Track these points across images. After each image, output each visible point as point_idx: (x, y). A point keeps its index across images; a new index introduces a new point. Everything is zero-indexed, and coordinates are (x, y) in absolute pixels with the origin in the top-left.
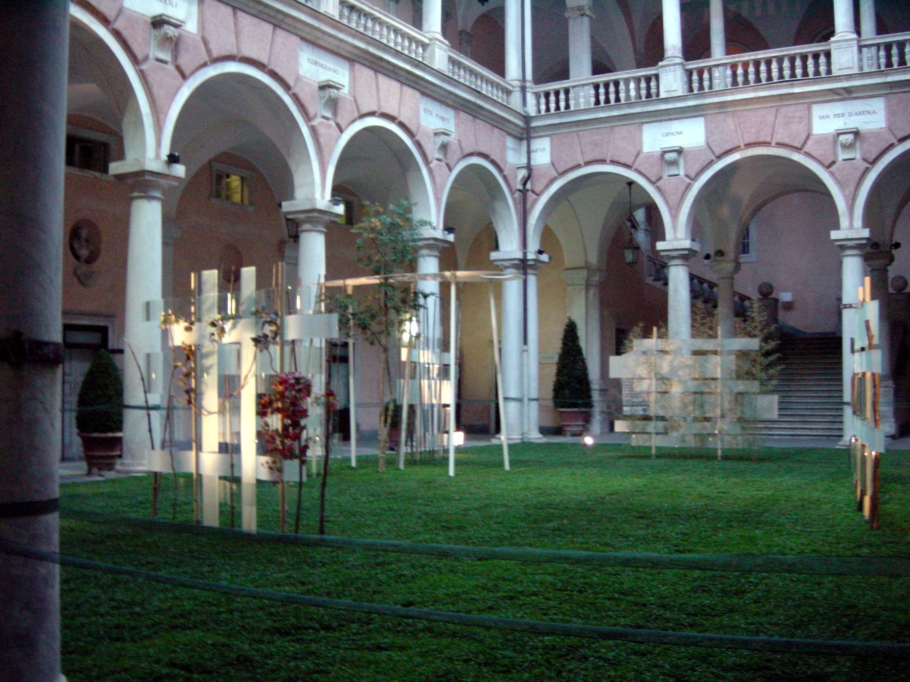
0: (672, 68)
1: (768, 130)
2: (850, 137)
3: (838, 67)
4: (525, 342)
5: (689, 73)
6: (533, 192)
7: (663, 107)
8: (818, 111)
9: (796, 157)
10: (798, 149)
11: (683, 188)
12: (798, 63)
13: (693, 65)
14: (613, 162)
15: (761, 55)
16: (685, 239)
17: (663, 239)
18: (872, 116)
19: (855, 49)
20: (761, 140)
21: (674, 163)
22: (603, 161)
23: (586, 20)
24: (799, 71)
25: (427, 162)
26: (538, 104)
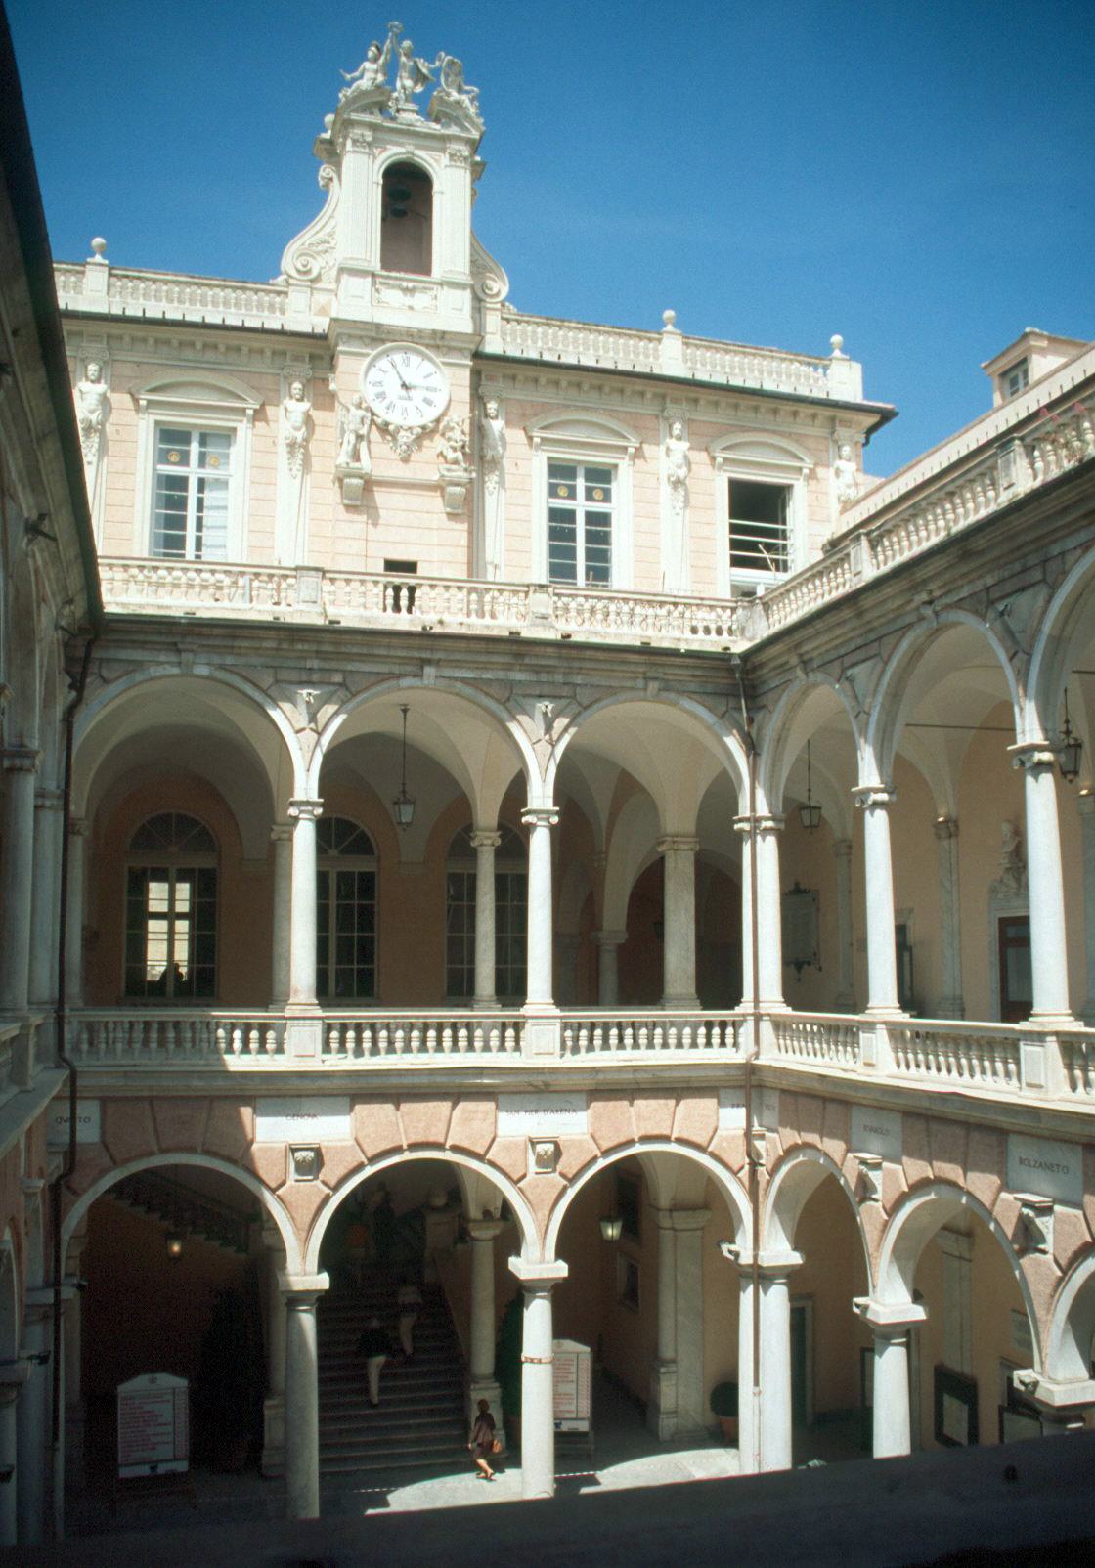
1: (442, 1127)
4: (55, 1437)
9: (474, 1164)
10: (480, 1157)
11: (317, 1201)
14: (208, 1152)
20: (432, 1139)
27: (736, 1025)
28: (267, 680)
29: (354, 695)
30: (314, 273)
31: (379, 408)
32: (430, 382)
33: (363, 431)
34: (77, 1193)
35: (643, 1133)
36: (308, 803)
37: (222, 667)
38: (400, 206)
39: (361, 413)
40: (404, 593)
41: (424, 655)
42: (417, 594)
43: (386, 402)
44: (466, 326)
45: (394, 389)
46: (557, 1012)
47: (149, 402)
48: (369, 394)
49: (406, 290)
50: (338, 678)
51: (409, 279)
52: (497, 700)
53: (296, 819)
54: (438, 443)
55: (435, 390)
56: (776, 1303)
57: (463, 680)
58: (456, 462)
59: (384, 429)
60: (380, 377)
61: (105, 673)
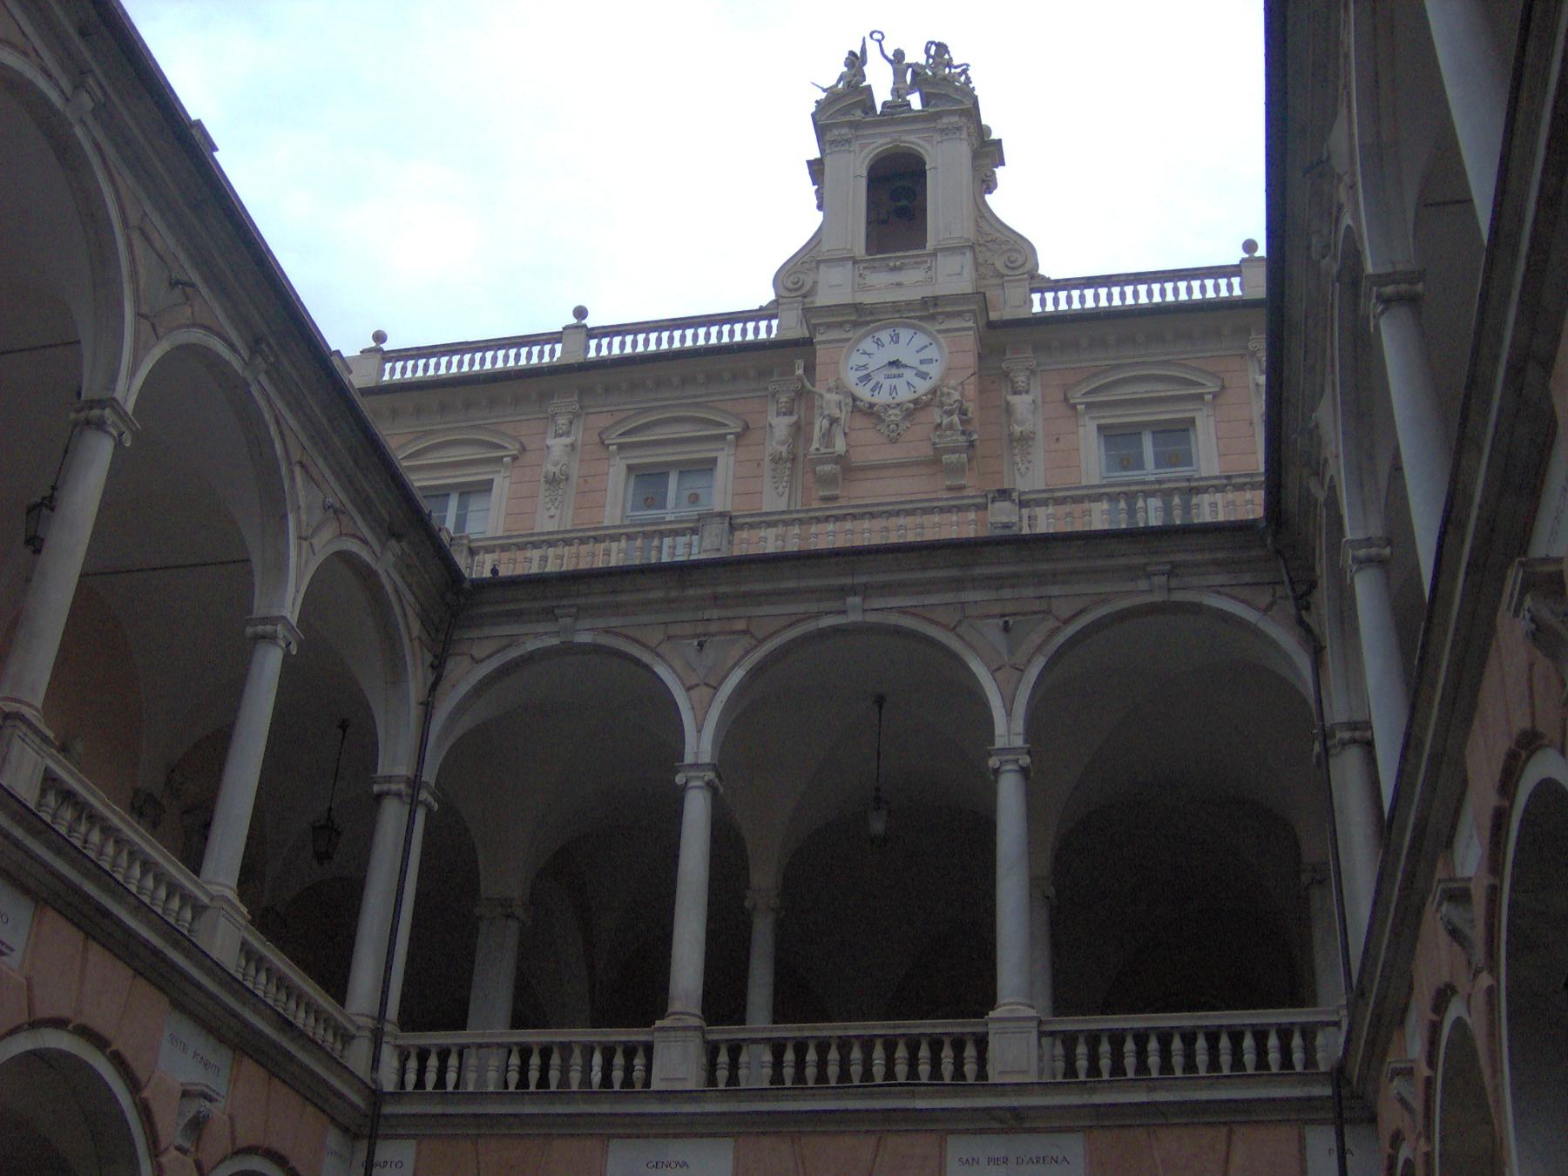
0: (679, 1034)
5: (712, 1050)
7: (655, 1108)
12: (924, 1052)
13: (721, 1033)
15: (856, 1029)
19: (1034, 1034)
23: (514, 925)
24: (924, 1069)
25: (155, 1149)
26: (403, 1072)
28: (654, 637)
29: (761, 642)
30: (807, 288)
31: (864, 393)
33: (843, 416)
36: (696, 766)
37: (607, 631)
38: (904, 203)
41: (847, 581)
44: (965, 285)
47: (621, 447)
48: (851, 378)
49: (894, 269)
52: (945, 626)
54: (936, 415)
55: (930, 361)
57: (903, 611)
59: (870, 412)
60: (863, 360)
61: (478, 652)
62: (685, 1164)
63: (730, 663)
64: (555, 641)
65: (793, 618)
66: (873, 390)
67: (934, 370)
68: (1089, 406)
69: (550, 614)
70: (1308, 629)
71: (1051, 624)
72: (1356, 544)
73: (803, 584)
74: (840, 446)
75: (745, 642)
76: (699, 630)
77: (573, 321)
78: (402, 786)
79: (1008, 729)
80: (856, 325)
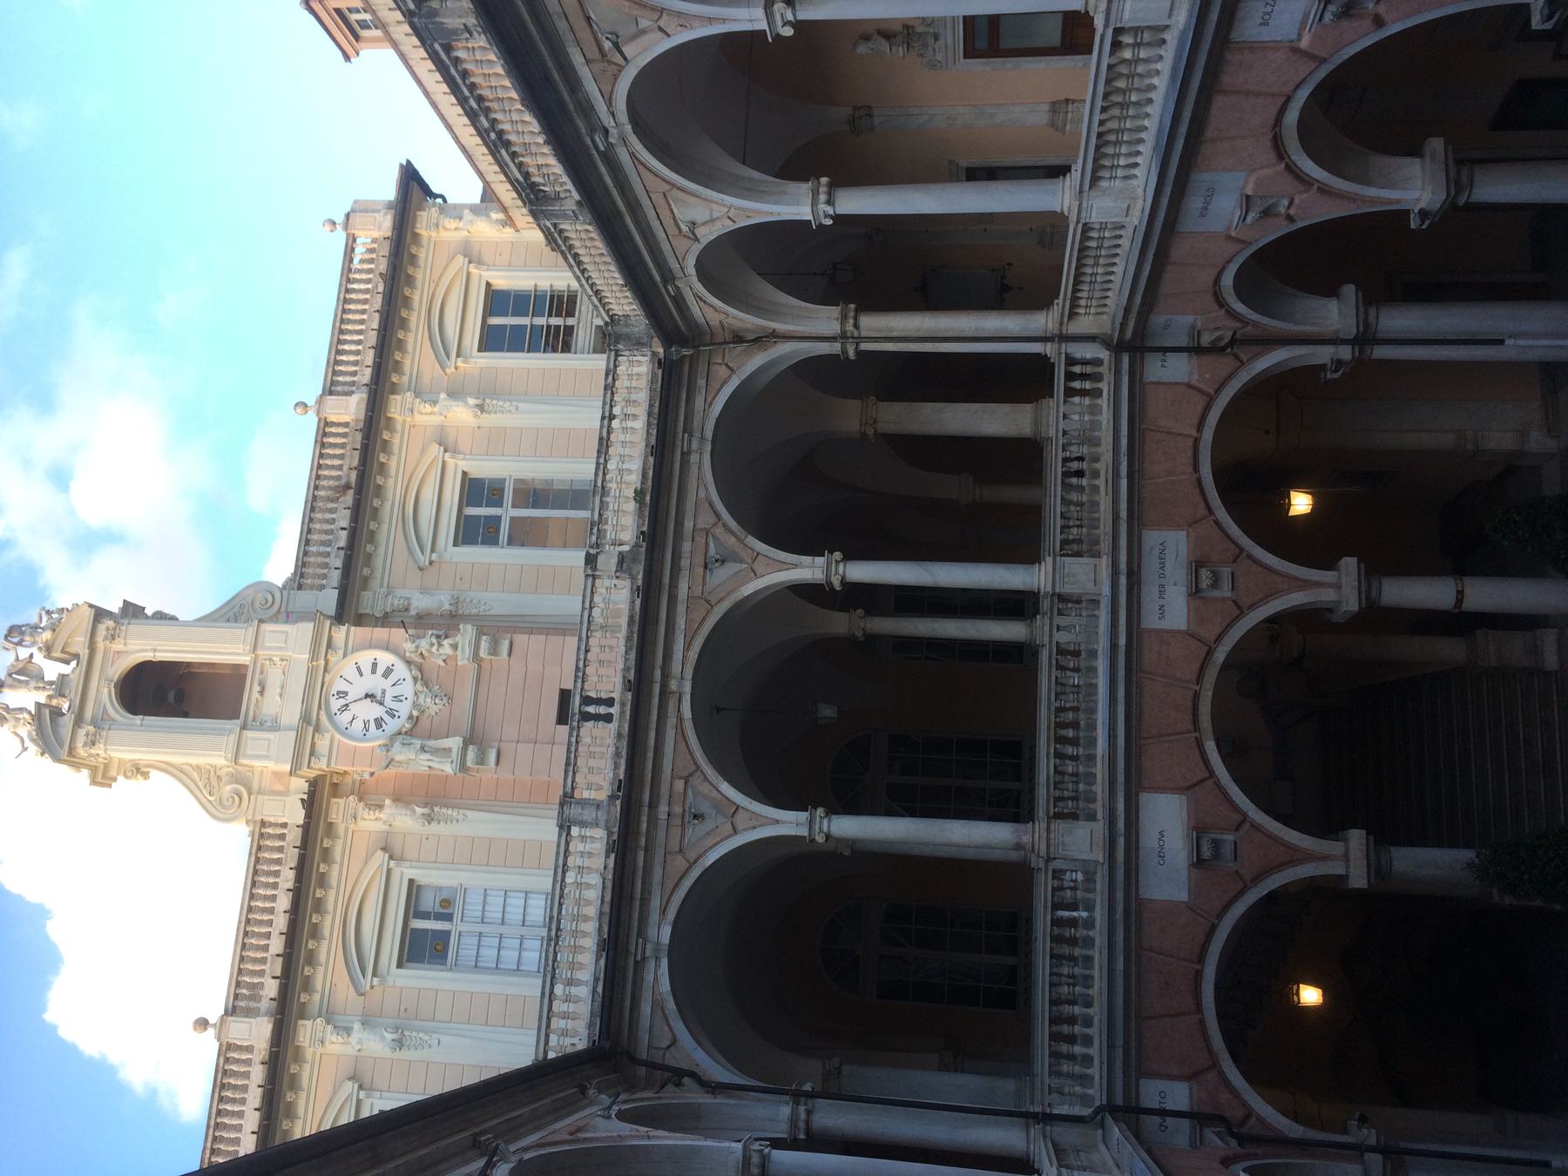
2: (1205, 574)
3: (1090, 586)
6: (1242, 1124)
8: (1151, 620)
9: (1220, 656)
10: (1210, 653)
14: (1201, 958)
16: (1346, 840)
17: (1343, 878)
18: (1170, 548)
21: (1217, 845)
22: (1198, 976)
23: (846, 1069)
27: (1071, 361)
28: (679, 863)
29: (698, 767)
31: (392, 725)
32: (367, 670)
34: (1249, 1114)
35: (1190, 470)
37: (664, 911)
38: (171, 696)
39: (397, 746)
40: (591, 709)
42: (593, 695)
43: (386, 718)
45: (372, 711)
46: (1049, 560)
49: (262, 693)
50: (679, 785)
51: (251, 693)
53: (828, 837)
55: (375, 665)
56: (1398, 320)
58: (455, 647)
59: (414, 721)
61: (665, 1043)
62: (1161, 833)
63: (715, 794)
64: (665, 962)
65: (680, 738)
66: (393, 716)
67: (386, 658)
68: (433, 551)
69: (639, 965)
70: (757, 340)
71: (719, 531)
72: (814, 204)
73: (654, 726)
74: (454, 743)
75: (696, 780)
76: (679, 822)
77: (211, 1032)
78: (802, 1109)
79: (808, 569)
80: (317, 729)
